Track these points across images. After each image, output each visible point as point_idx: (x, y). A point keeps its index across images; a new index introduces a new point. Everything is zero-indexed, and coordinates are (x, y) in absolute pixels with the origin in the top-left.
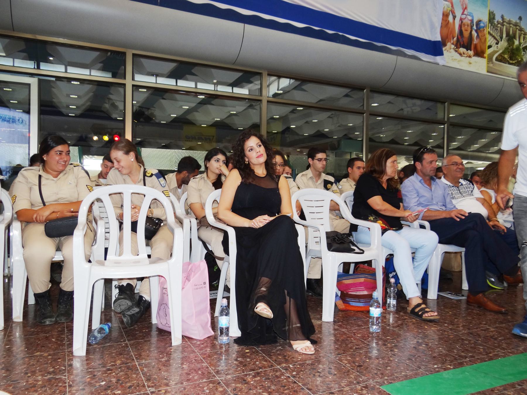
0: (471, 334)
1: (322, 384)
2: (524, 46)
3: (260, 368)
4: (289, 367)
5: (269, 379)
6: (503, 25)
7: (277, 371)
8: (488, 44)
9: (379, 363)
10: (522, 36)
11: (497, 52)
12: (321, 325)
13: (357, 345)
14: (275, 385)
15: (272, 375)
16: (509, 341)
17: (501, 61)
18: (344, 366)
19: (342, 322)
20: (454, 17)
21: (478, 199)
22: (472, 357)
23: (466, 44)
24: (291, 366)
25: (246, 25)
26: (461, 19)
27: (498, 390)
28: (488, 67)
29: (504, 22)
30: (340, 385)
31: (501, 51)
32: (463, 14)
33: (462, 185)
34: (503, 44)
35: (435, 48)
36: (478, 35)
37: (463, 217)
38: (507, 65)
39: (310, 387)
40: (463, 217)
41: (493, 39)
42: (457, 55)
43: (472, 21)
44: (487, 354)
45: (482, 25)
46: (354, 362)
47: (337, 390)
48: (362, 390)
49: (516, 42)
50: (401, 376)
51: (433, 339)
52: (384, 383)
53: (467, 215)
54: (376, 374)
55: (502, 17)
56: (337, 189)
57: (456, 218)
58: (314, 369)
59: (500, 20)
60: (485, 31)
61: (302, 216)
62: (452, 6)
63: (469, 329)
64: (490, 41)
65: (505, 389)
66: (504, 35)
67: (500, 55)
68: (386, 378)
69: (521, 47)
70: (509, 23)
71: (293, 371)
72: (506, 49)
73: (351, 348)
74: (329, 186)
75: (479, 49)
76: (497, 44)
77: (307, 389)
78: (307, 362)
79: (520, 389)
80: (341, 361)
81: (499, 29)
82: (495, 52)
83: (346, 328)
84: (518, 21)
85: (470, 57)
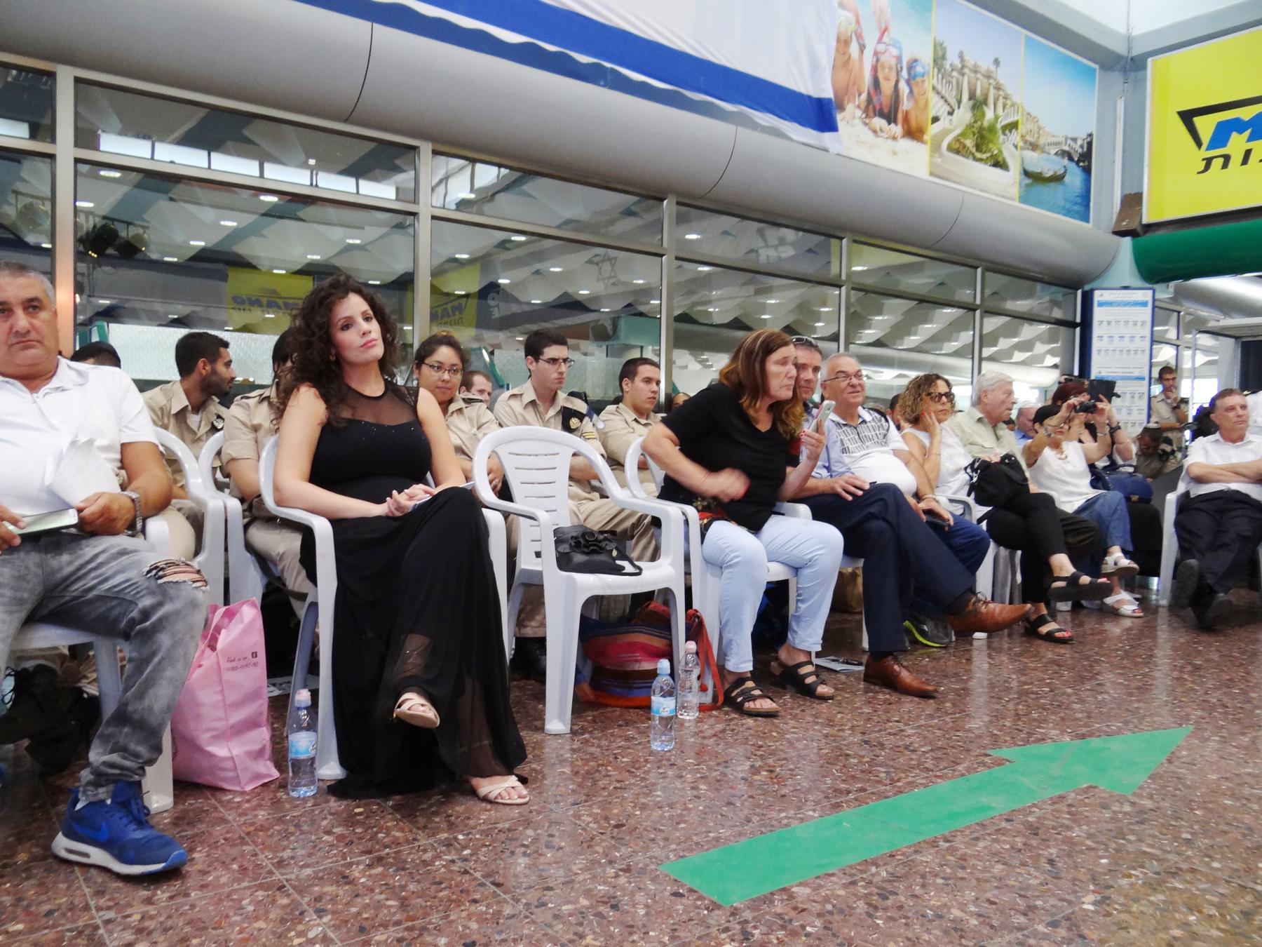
0: (866, 742)
1: (527, 871)
2: (1004, 123)
3: (386, 847)
4: (456, 839)
5: (404, 869)
6: (963, 75)
7: (425, 851)
8: (931, 114)
9: (662, 817)
10: (1001, 101)
11: (951, 131)
12: (543, 741)
13: (619, 781)
14: (418, 881)
15: (413, 860)
16: (939, 754)
17: (958, 152)
18: (584, 829)
19: (591, 732)
20: (862, 48)
21: (897, 453)
22: (863, 790)
23: (886, 110)
24: (461, 837)
25: (378, 28)
26: (876, 53)
27: (904, 854)
28: (932, 164)
29: (963, 67)
30: (570, 870)
31: (958, 132)
32: (880, 41)
33: (864, 422)
35: (821, 115)
36: (911, 91)
37: (860, 493)
38: (970, 162)
39: (499, 879)
40: (860, 493)
41: (942, 102)
43: (899, 59)
44: (893, 782)
45: (919, 69)
46: (606, 819)
47: (560, 880)
48: (617, 876)
49: (989, 114)
50: (708, 842)
51: (785, 759)
52: (668, 858)
53: (867, 487)
54: (653, 840)
55: (961, 56)
56: (594, 430)
57: (844, 494)
58: (512, 839)
59: (958, 63)
60: (926, 84)
61: (504, 492)
62: (858, 22)
63: (863, 733)
64: (936, 106)
65: (916, 852)
66: (965, 97)
67: (957, 139)
68: (673, 846)
69: (999, 126)
71: (465, 848)
72: (970, 126)
73: (604, 789)
74: (574, 422)
75: (913, 123)
76: (951, 113)
77: (495, 884)
78: (500, 826)
79: (948, 849)
80: (578, 817)
81: (954, 81)
82: (946, 132)
83: (599, 746)
84: (993, 68)
85: (894, 138)
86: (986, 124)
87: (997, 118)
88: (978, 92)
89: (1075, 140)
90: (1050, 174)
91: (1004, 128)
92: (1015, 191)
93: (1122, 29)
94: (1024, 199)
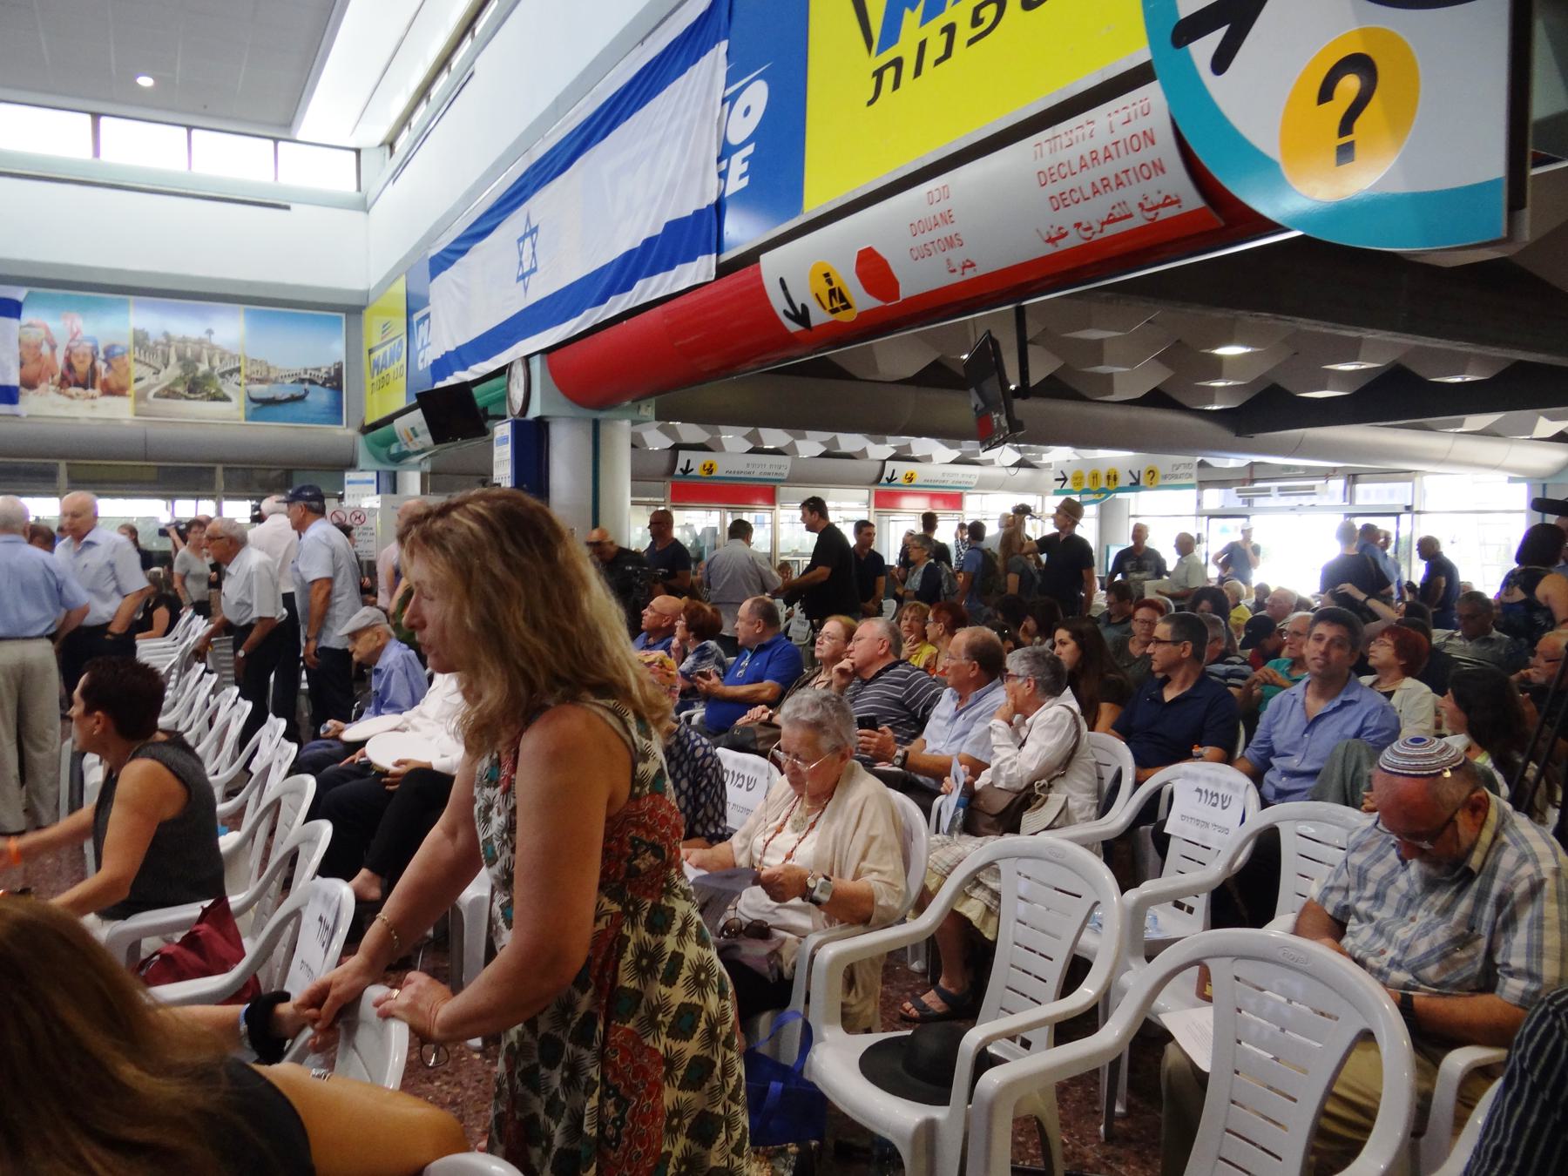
8: (134, 376)
17: (167, 397)
26: (69, 349)
31: (167, 383)
34: (173, 372)
36: (109, 366)
38: (183, 402)
42: (63, 400)
43: (95, 349)
45: (118, 350)
64: (136, 370)
66: (173, 360)
70: (184, 341)
75: (113, 385)
76: (157, 372)
82: (151, 386)
85: (92, 398)
86: (199, 374)
87: (212, 368)
88: (189, 354)
89: (319, 369)
90: (287, 396)
91: (222, 375)
92: (241, 414)
93: (361, 287)
94: (247, 419)
